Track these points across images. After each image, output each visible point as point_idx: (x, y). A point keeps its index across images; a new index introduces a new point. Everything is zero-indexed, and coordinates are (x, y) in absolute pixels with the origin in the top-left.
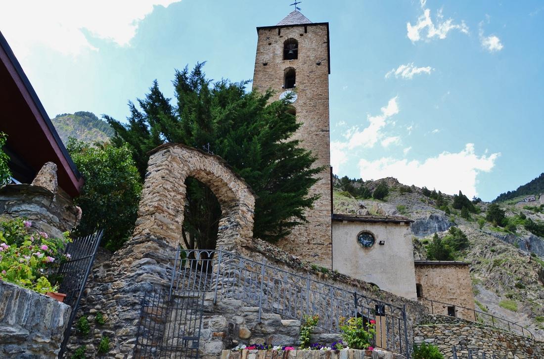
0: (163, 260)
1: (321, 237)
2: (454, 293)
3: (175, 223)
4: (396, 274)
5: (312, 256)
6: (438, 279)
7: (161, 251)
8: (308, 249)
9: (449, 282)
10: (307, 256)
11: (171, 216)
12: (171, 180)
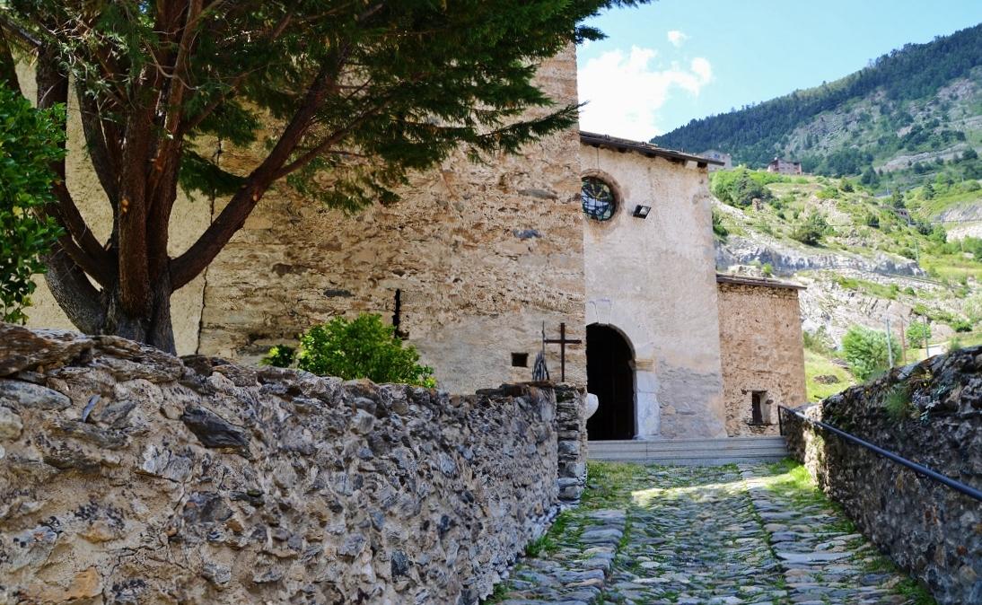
1: (545, 170)
2: (766, 359)
4: (673, 306)
5: (515, 233)
6: (734, 318)
8: (502, 210)
9: (756, 330)
10: (500, 234)
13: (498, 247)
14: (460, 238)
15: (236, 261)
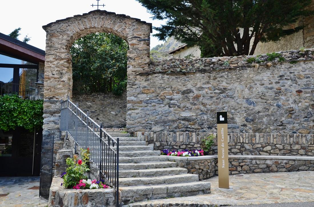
0: (54, 113)
3: (61, 83)
7: (53, 106)
11: (57, 79)
12: (52, 52)
15: (310, 45)
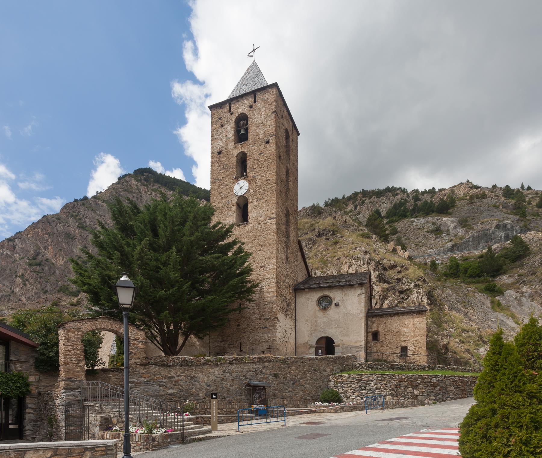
4: (348, 328)
10: (259, 329)
13: (259, 331)
14: (252, 331)
